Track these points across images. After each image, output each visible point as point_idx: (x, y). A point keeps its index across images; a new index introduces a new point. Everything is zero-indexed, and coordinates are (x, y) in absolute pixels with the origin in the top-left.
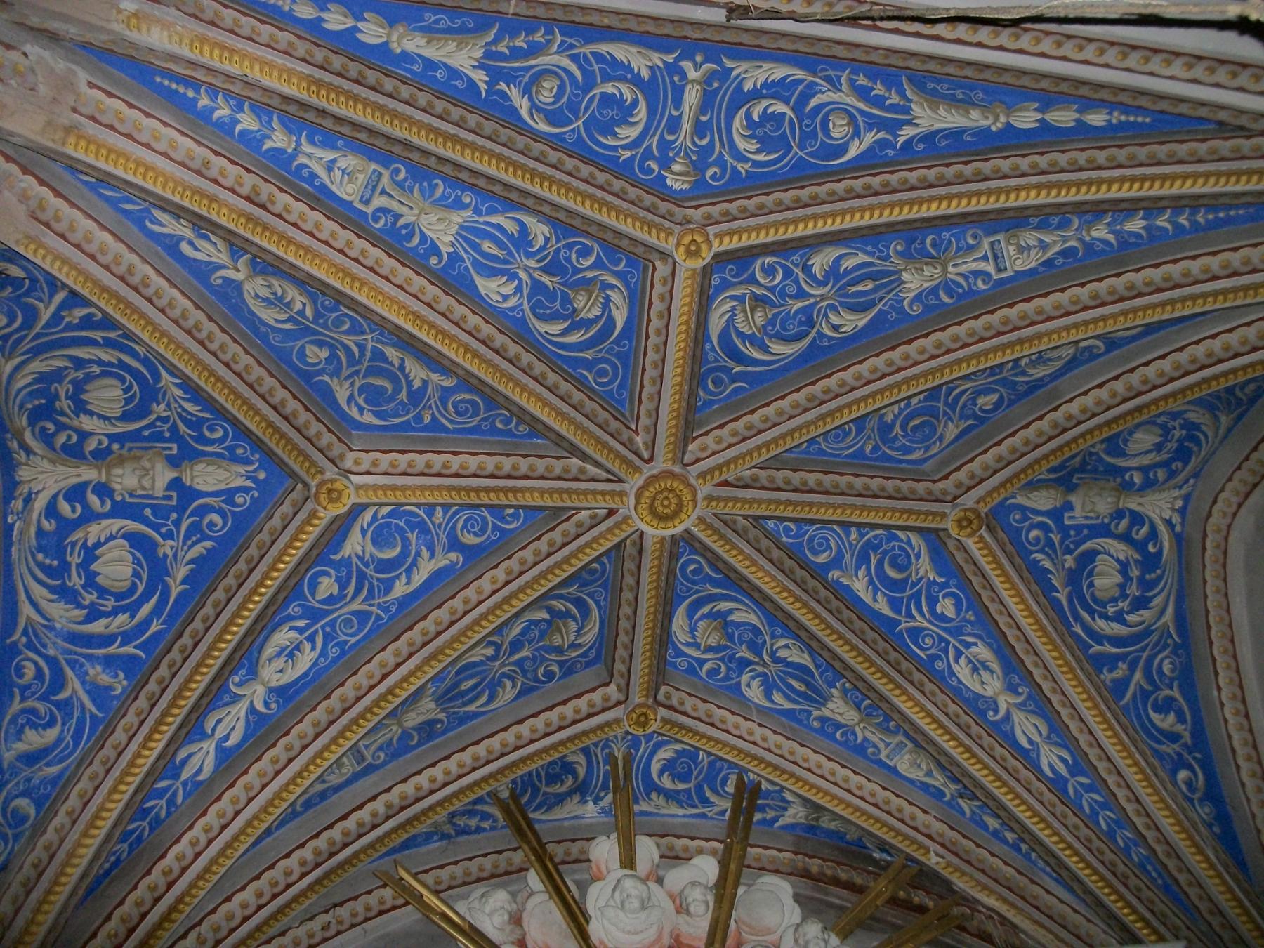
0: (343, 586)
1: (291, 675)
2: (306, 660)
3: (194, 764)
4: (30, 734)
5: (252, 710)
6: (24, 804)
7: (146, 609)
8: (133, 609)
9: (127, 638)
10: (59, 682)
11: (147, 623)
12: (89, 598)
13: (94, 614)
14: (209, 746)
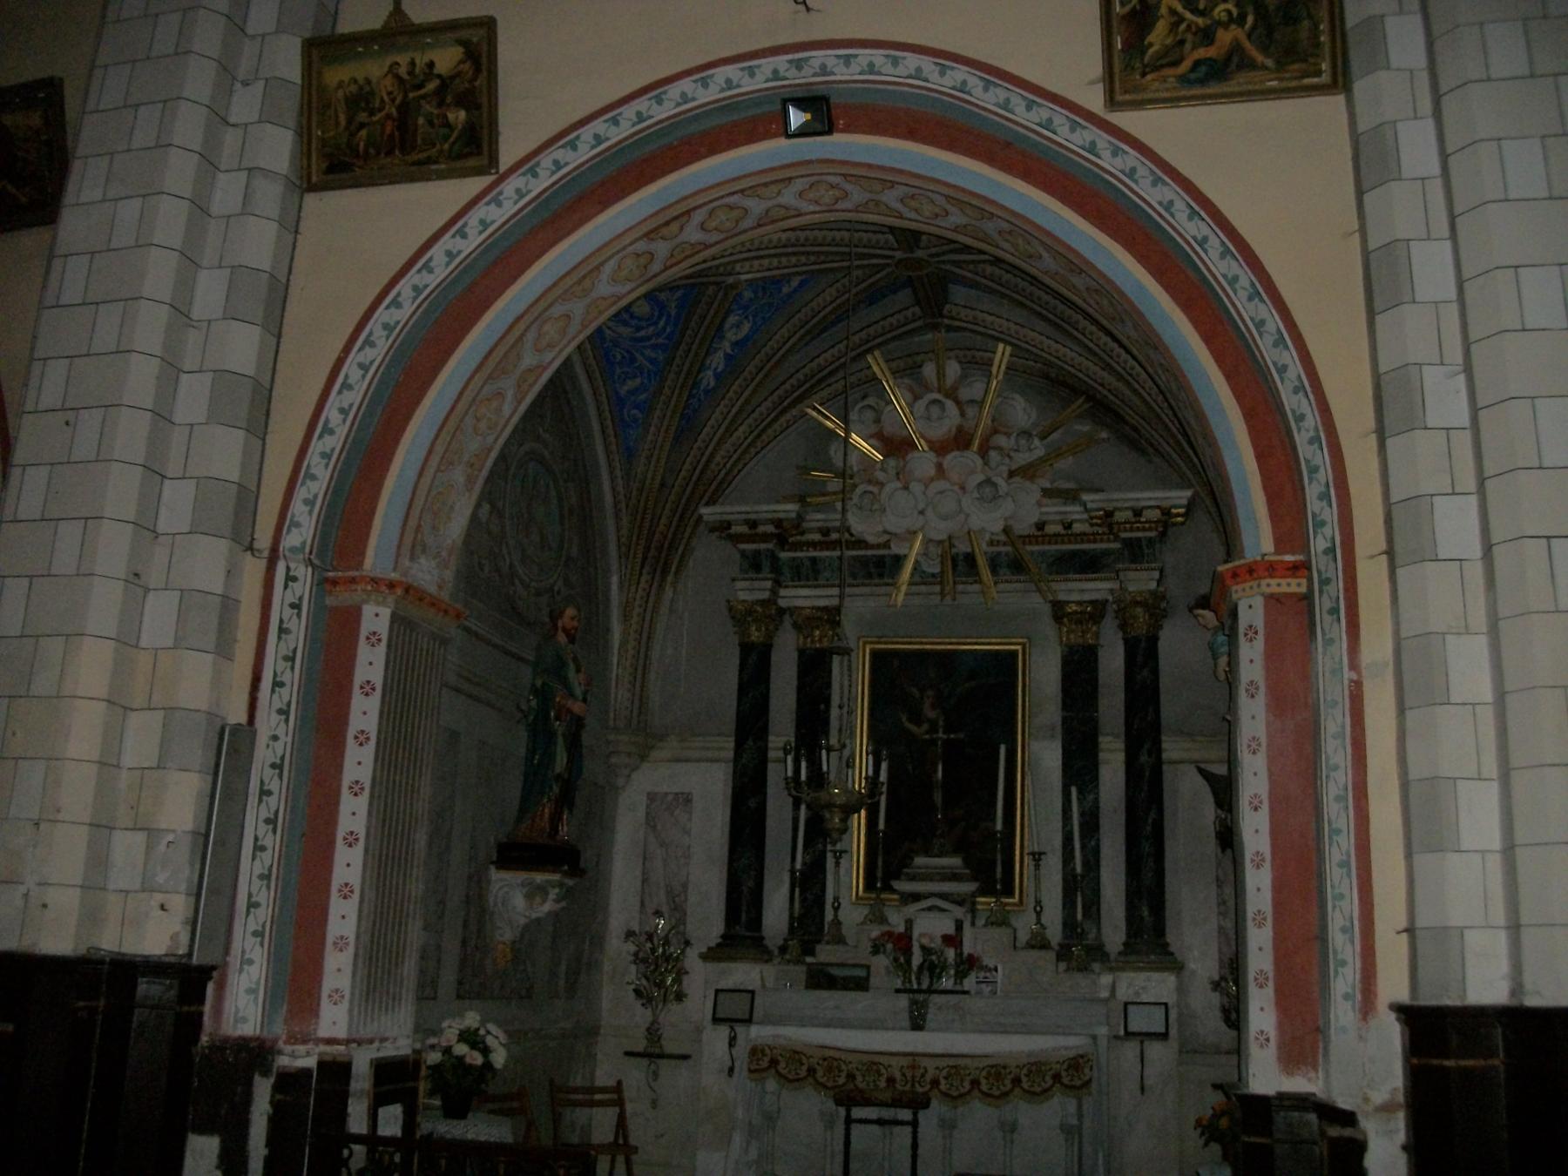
0: (755, 292)
1: (741, 335)
2: (746, 327)
3: (705, 382)
4: (630, 383)
5: (726, 355)
6: (635, 412)
7: (662, 323)
8: (656, 323)
9: (658, 335)
10: (633, 360)
11: (664, 329)
12: (634, 322)
13: (639, 329)
14: (710, 373)
